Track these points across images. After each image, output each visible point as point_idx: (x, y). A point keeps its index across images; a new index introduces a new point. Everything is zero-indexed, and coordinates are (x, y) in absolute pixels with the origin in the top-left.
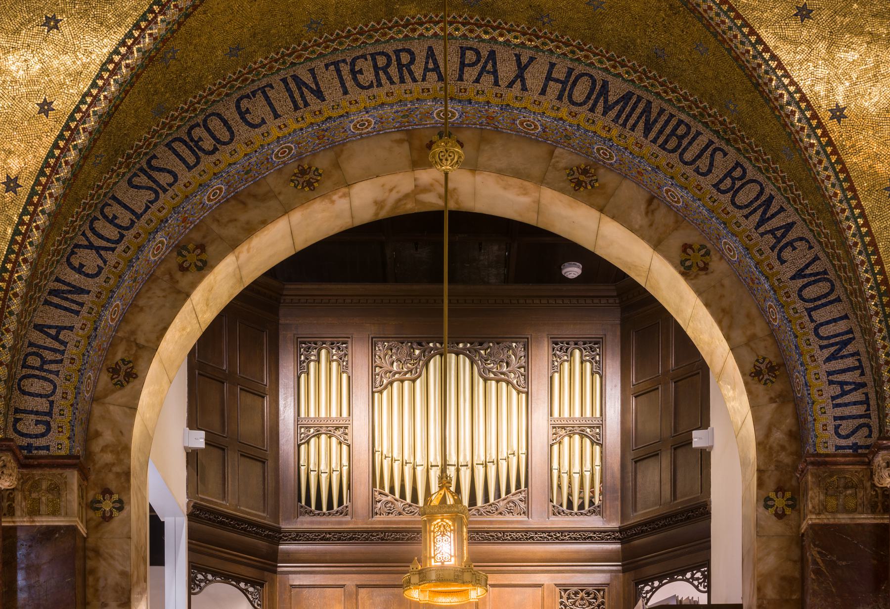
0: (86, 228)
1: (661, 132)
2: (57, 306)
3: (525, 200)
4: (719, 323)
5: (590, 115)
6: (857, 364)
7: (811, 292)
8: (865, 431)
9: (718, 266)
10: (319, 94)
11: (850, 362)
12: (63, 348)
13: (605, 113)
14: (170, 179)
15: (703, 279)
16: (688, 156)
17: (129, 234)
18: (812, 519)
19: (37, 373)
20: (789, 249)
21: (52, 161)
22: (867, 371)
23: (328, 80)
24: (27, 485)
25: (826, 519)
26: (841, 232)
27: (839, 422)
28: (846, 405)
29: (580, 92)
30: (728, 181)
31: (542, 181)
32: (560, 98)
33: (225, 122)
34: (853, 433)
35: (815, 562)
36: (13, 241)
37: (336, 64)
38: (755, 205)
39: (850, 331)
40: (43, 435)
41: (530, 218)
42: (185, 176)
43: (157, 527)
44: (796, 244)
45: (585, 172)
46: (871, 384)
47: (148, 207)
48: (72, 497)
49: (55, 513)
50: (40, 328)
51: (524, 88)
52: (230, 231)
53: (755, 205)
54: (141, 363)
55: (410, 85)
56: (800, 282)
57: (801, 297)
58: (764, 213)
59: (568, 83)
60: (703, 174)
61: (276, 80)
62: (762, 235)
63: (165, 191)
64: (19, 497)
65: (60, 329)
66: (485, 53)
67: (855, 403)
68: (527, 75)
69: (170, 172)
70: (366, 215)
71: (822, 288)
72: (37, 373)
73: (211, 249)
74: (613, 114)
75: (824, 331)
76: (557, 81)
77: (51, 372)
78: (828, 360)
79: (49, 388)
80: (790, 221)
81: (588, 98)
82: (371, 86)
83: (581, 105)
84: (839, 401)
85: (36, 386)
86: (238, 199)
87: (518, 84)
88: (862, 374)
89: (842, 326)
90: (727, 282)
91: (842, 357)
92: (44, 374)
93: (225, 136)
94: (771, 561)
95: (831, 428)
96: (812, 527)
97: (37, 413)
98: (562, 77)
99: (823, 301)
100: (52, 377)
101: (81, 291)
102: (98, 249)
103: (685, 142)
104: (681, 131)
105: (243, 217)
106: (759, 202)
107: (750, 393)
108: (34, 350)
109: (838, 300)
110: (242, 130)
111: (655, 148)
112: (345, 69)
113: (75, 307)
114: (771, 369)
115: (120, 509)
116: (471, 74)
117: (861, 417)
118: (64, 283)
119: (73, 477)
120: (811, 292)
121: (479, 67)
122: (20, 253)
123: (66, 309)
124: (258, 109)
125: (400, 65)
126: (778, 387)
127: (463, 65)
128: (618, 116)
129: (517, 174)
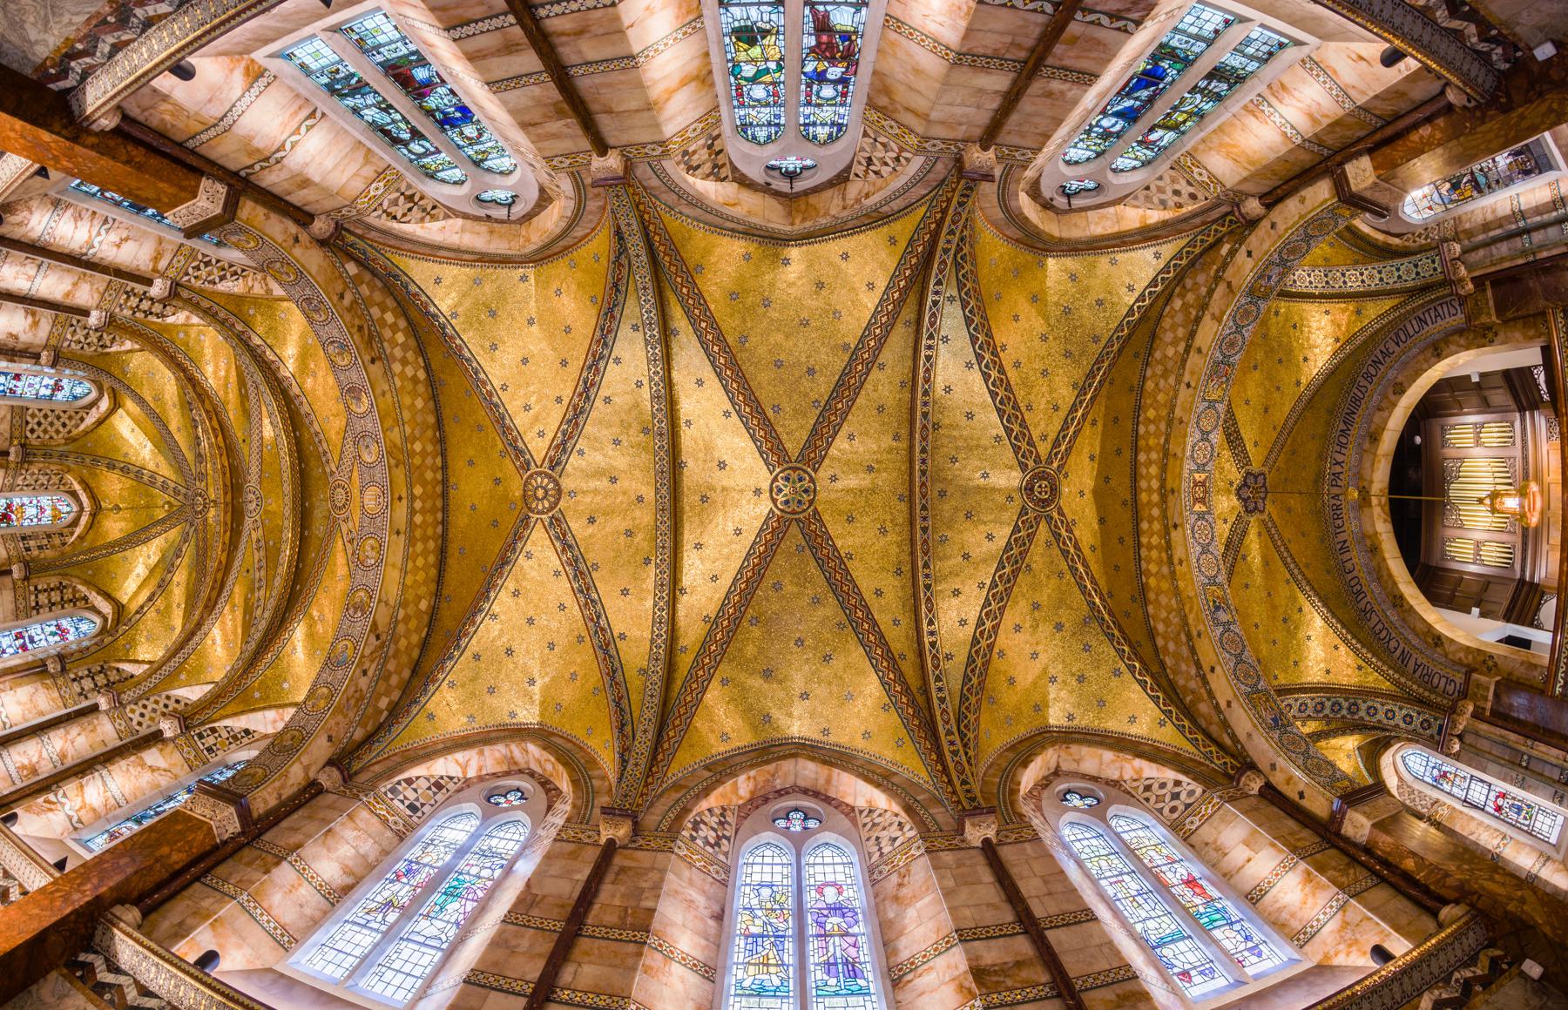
3: (1383, 461)
10: (1345, 541)
18: (1494, 318)
23: (1341, 537)
24: (1474, 698)
25: (1493, 311)
31: (1375, 454)
41: (1390, 459)
42: (1368, 599)
43: (1510, 640)
48: (1483, 679)
49: (1488, 689)
52: (1390, 583)
70: (1389, 527)
86: (1379, 578)
93: (1356, 581)
94: (1517, 335)
110: (1355, 573)
116: (1340, 483)
119: (1475, 676)
124: (1349, 565)
129: (1373, 464)
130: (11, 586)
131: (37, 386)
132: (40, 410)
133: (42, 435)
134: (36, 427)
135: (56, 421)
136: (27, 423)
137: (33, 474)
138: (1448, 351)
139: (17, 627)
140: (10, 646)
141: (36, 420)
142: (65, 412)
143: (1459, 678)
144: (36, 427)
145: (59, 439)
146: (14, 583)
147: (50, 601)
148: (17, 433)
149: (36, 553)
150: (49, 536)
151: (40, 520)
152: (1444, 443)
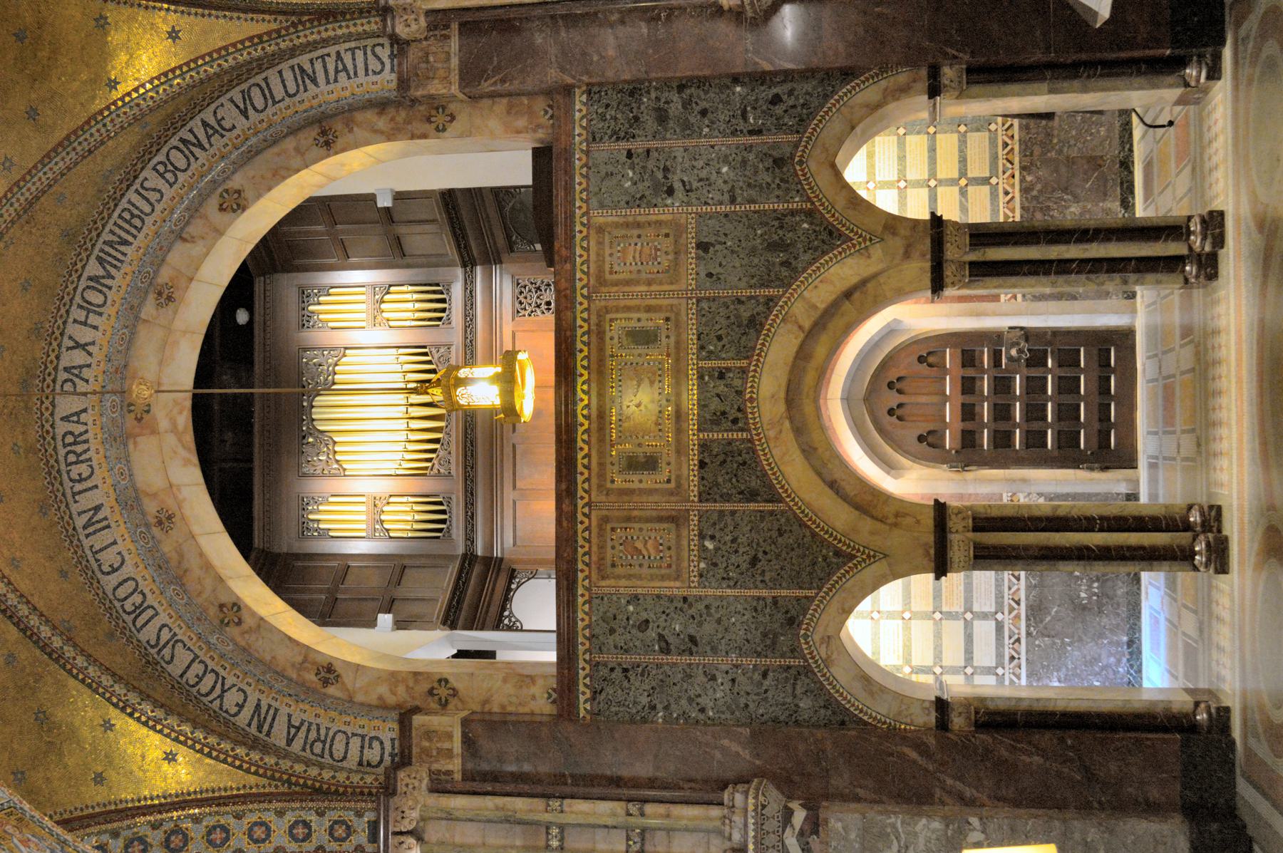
0: (205, 700)
1: (128, 232)
2: (271, 726)
4: (284, 178)
5: (114, 289)
6: (320, 60)
7: (259, 102)
8: (378, 49)
9: (237, 181)
10: (97, 508)
11: (318, 66)
12: (306, 724)
13: (113, 278)
14: (166, 630)
15: (248, 194)
16: (147, 209)
17: (211, 665)
18: (455, 89)
19: (327, 746)
20: (223, 123)
21: (151, 723)
22: (325, 51)
23: (87, 501)
25: (455, 77)
26: (209, 78)
27: (370, 72)
28: (355, 67)
29: (96, 298)
30: (168, 176)
31: (169, 330)
32: (100, 314)
33: (120, 584)
34: (379, 59)
35: (495, 83)
36: (216, 758)
37: (74, 495)
38: (187, 152)
39: (292, 68)
40: (382, 743)
42: (163, 618)
44: (219, 118)
45: (160, 294)
46: (337, 48)
47: (189, 649)
48: (436, 721)
49: (449, 736)
50: (290, 741)
51: (93, 343)
52: (208, 583)
53: (187, 152)
54: (319, 659)
55: (90, 435)
56: (251, 112)
57: (262, 111)
58: (194, 145)
59: (88, 307)
60: (162, 197)
61: (86, 543)
62: (211, 145)
63: (175, 634)
64: (435, 766)
65: (290, 725)
66: (66, 376)
67: (354, 59)
68: (82, 341)
69: (160, 630)
71: (256, 93)
72: (327, 746)
73: (224, 599)
74: (113, 271)
75: (292, 88)
76: (87, 317)
77: (327, 735)
78: (316, 84)
79: (340, 737)
80: (200, 124)
81: (100, 291)
82: (91, 466)
83: (106, 297)
84: (352, 73)
85: (339, 748)
87: (90, 348)
88: (328, 55)
89: (288, 75)
90: (251, 173)
91: (314, 72)
92: (329, 740)
93: (131, 584)
94: (494, 124)
95: (375, 78)
96: (461, 88)
97: (362, 747)
98: (84, 313)
99: (266, 92)
100: (331, 734)
101: (258, 706)
102: (224, 691)
103: (136, 212)
104: (127, 215)
105: (197, 572)
106: (185, 150)
107: (344, 150)
108: (308, 747)
109: (266, 79)
110: (128, 570)
111: (141, 236)
112: (78, 487)
113: (272, 712)
114: (324, 133)
115: (447, 681)
117: (365, 54)
118: (252, 719)
119: (417, 720)
120: (259, 102)
121: (77, 380)
122: (226, 753)
123: (273, 719)
125: (75, 443)
126: (338, 126)
127: (75, 393)
128: (115, 267)
138: (350, 138)
143: (388, 732)
152: (305, 321)
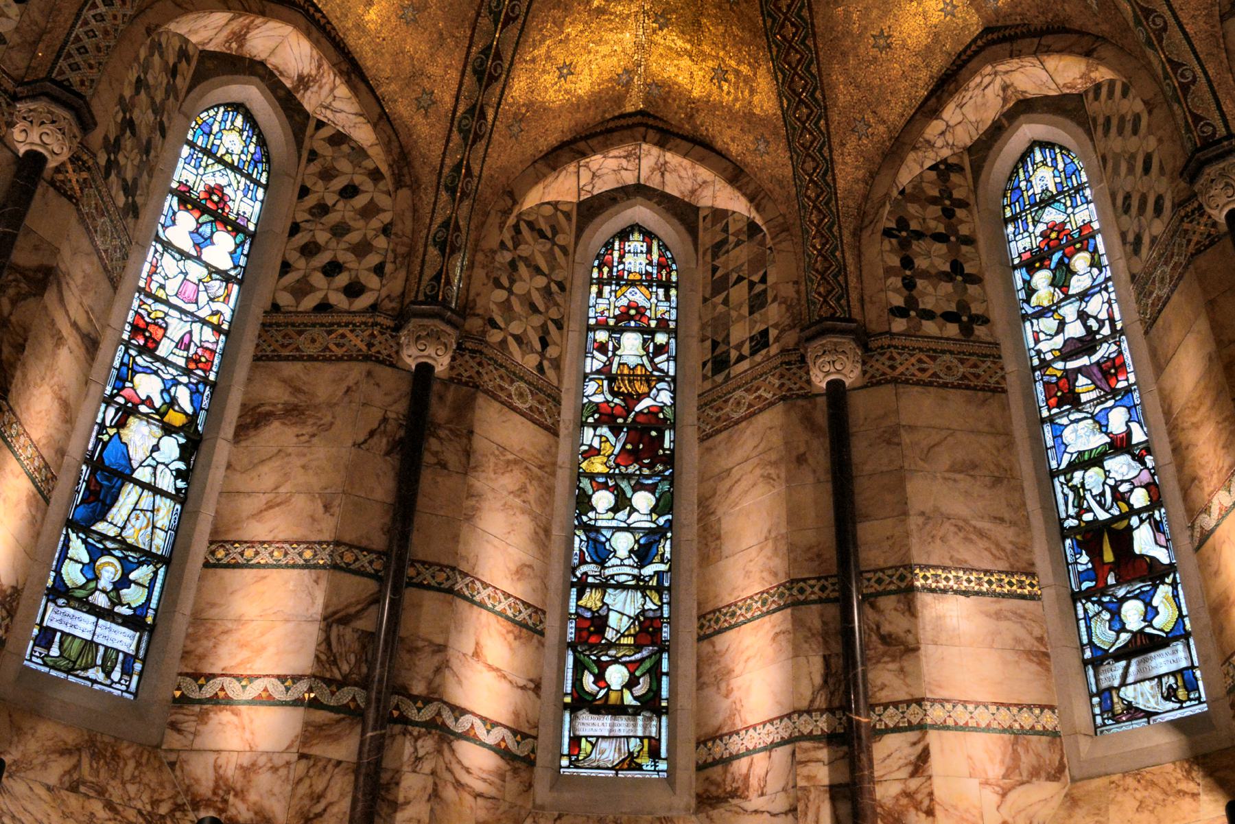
130: (887, 391)
131: (196, 271)
132: (286, 267)
133: (373, 260)
134: (342, 279)
135: (333, 218)
136: (324, 307)
137: (506, 306)
139: (1030, 396)
140: (1101, 425)
141: (318, 279)
142: (304, 192)
144: (342, 279)
145: (390, 205)
146: (872, 382)
147: (947, 277)
148: (357, 341)
149: (774, 312)
150: (720, 285)
151: (663, 325)
